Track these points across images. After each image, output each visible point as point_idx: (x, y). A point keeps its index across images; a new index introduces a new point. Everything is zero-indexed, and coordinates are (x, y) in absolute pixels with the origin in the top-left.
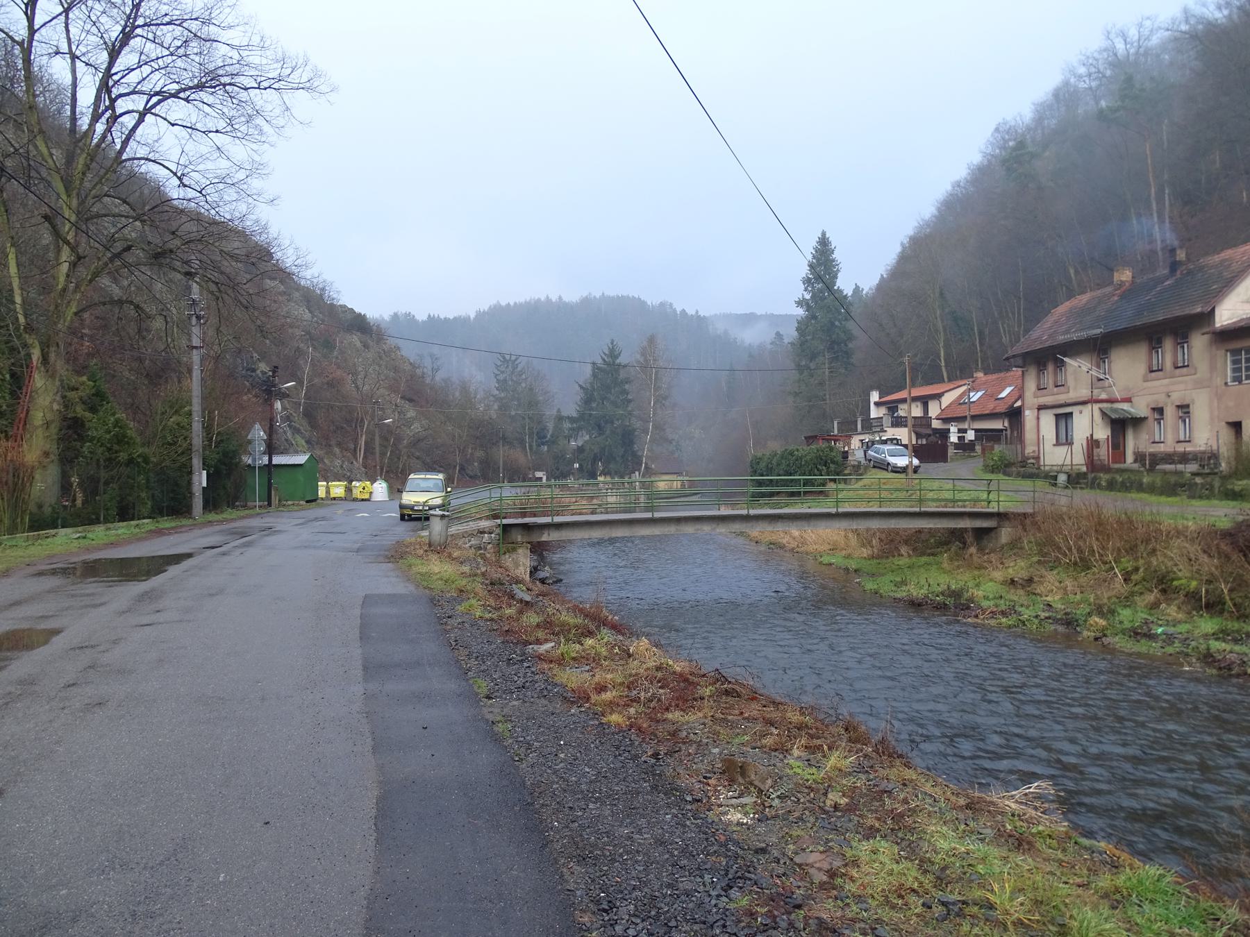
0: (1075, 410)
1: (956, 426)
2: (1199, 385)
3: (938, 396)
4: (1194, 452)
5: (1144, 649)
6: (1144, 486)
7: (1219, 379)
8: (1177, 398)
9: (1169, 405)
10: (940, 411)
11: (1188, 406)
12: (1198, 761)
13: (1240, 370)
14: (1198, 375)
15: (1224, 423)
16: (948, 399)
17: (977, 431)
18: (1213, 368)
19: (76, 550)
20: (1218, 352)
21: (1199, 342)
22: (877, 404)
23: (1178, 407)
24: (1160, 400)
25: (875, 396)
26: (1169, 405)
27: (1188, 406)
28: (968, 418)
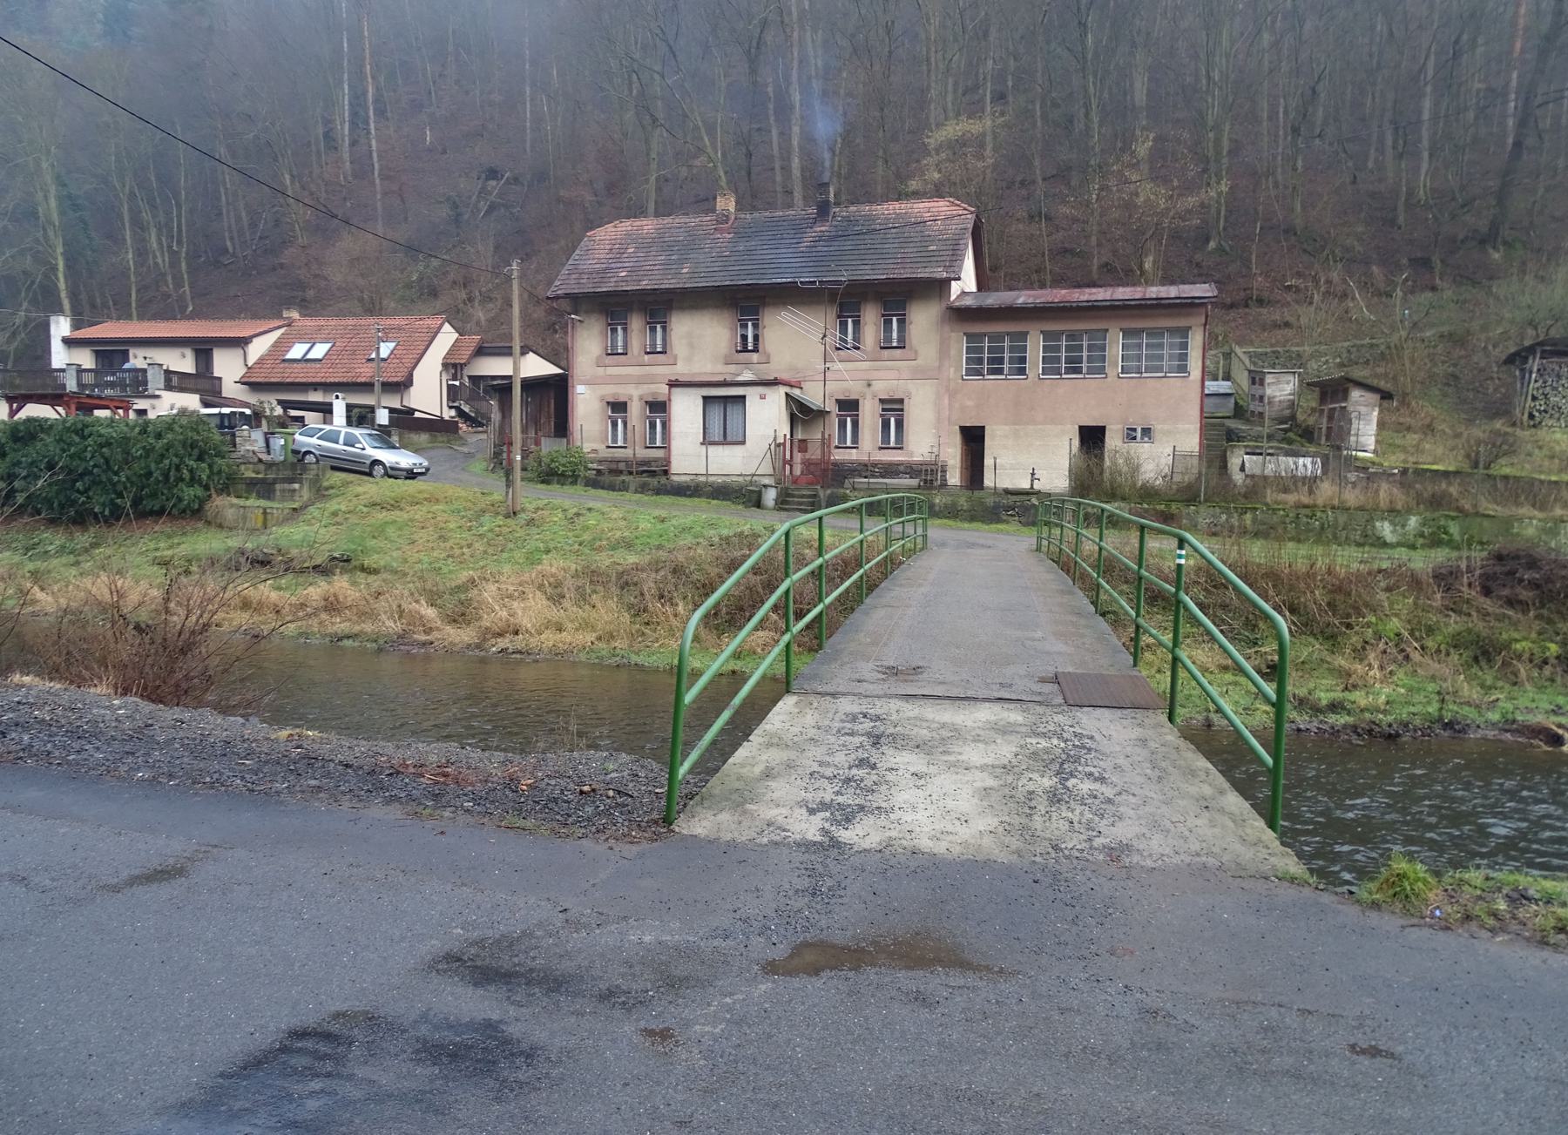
0: (752, 394)
1: (344, 399)
2: (921, 375)
3: (241, 343)
4: (908, 462)
5: (363, 746)
6: (937, 508)
7: (952, 370)
8: (883, 388)
9: (869, 397)
10: (245, 370)
11: (901, 401)
12: (1489, 830)
13: (980, 361)
14: (919, 362)
15: (957, 427)
16: (258, 348)
17: (392, 410)
18: (943, 353)
19: (257, 765)
20: (953, 334)
21: (923, 319)
22: (69, 342)
23: (882, 401)
24: (852, 389)
25: (61, 327)
26: (869, 397)
27: (901, 401)
28: (377, 387)
